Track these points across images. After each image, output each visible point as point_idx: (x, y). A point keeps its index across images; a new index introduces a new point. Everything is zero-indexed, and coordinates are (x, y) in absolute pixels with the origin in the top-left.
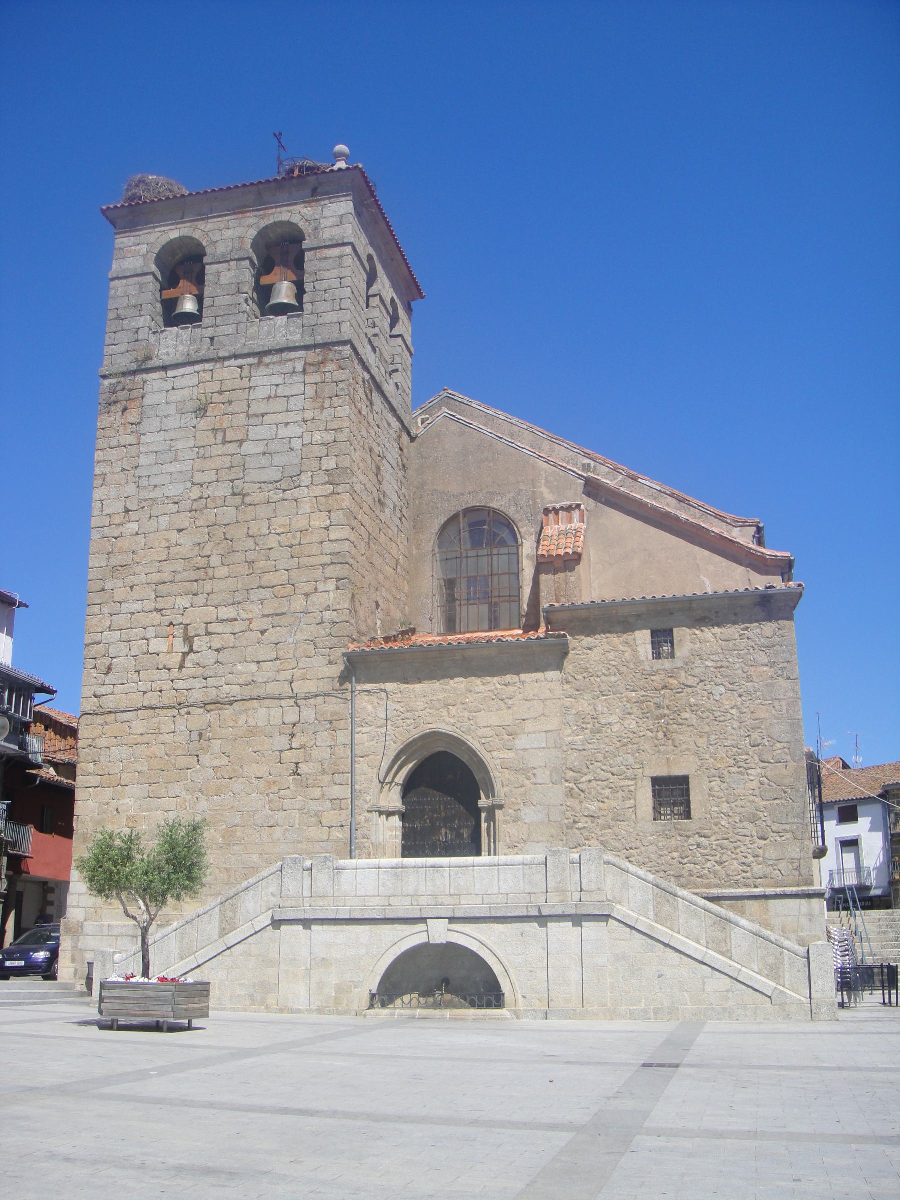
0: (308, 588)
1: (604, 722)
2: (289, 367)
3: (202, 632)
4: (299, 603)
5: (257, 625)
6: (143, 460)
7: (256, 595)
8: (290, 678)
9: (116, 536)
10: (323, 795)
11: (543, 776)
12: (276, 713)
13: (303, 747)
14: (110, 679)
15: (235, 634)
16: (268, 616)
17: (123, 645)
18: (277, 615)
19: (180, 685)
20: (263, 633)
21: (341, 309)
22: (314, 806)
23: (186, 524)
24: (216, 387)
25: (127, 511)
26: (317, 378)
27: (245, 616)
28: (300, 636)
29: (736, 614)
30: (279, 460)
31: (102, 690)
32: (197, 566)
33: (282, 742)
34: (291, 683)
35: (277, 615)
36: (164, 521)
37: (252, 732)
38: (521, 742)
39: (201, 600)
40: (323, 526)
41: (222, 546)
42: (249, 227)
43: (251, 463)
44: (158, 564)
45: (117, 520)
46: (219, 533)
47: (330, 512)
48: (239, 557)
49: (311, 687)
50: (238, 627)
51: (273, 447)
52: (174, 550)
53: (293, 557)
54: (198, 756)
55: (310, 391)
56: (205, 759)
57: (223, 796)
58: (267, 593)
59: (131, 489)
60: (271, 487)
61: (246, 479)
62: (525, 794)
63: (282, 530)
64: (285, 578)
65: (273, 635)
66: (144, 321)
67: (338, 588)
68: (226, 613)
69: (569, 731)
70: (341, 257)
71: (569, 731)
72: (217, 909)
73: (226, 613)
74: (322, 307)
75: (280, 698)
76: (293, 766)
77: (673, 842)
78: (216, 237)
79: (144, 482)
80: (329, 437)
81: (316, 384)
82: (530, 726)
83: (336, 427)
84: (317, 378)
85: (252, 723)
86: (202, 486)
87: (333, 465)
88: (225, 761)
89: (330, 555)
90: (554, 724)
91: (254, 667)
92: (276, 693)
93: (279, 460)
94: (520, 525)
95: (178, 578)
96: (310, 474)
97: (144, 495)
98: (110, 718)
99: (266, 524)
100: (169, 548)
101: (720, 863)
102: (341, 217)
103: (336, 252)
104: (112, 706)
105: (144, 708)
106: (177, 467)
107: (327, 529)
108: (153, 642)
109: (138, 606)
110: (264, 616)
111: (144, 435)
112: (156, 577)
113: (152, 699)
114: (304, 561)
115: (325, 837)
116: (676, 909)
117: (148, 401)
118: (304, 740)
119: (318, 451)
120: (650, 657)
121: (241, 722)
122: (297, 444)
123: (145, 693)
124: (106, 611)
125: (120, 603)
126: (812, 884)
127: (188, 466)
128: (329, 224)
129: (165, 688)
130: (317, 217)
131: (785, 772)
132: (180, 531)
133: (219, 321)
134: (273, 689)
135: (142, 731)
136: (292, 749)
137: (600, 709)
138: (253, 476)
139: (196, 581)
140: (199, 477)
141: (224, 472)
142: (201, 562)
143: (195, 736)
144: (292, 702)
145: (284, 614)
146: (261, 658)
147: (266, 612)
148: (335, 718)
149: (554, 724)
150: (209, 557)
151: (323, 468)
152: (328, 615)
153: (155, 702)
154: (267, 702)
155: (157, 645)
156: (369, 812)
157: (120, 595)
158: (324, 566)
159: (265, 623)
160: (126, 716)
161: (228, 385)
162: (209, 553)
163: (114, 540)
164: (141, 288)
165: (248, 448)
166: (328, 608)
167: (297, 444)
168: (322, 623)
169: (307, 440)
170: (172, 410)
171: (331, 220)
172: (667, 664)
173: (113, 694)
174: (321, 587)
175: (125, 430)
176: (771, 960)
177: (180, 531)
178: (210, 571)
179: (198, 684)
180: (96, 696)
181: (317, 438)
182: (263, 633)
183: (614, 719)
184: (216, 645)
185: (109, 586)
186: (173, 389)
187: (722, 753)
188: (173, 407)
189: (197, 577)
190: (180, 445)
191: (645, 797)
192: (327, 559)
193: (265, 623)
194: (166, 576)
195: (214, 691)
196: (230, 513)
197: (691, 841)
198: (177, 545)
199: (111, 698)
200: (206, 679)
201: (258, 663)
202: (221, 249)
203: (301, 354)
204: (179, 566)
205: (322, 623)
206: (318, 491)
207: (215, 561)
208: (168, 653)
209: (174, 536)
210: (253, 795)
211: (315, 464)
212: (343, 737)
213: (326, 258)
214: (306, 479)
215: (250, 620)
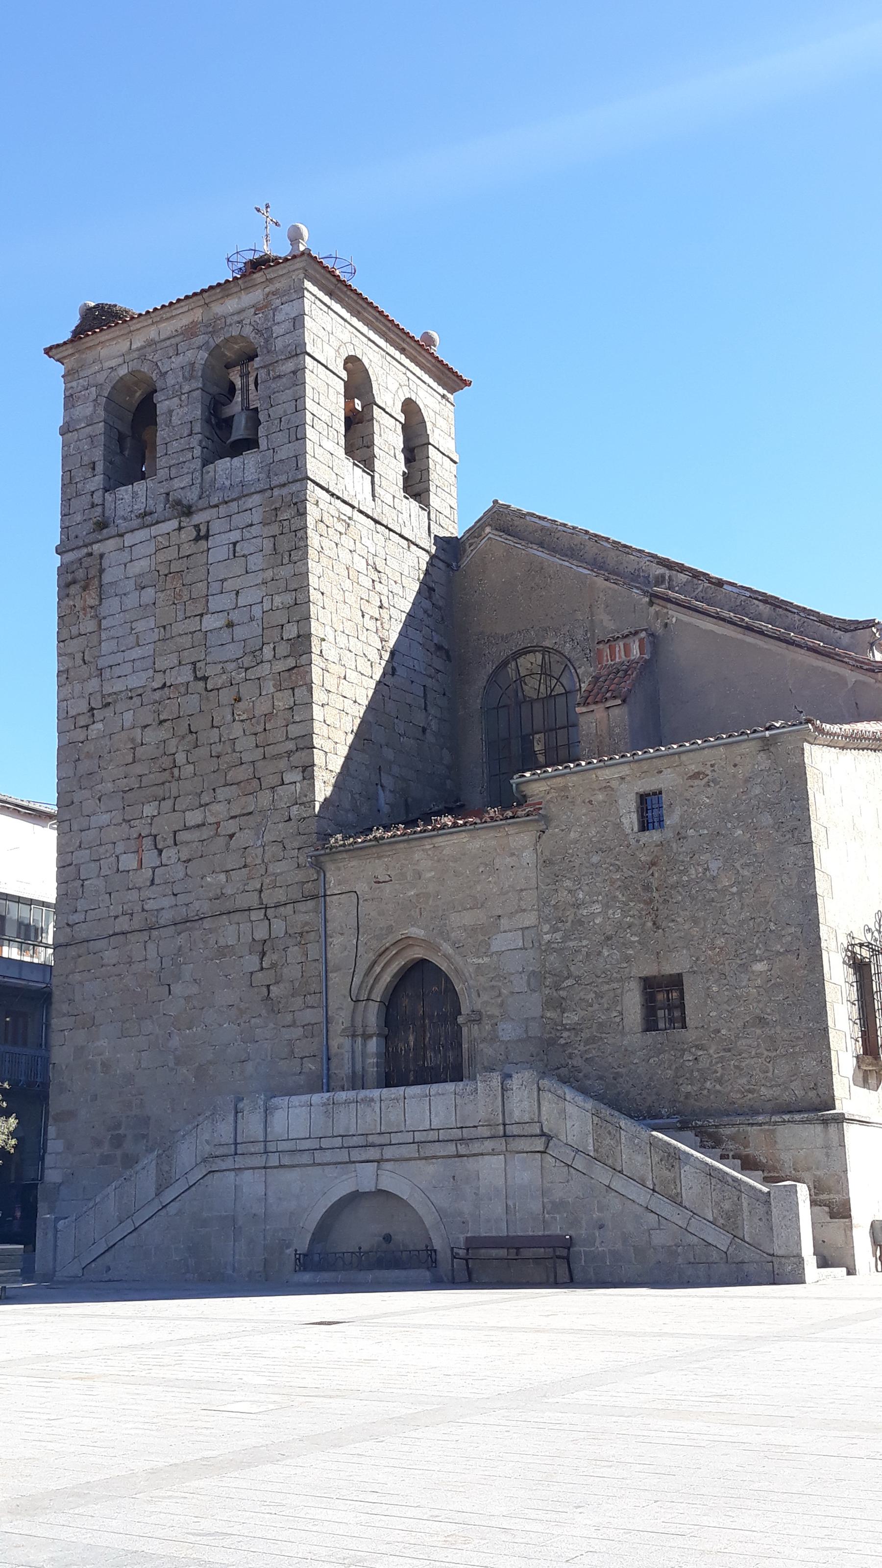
0: (274, 780)
2: (246, 518)
4: (265, 799)
6: (105, 647)
8: (259, 886)
9: (82, 740)
10: (294, 1021)
11: (520, 983)
13: (274, 966)
16: (232, 818)
17: (93, 865)
18: (244, 815)
20: (231, 836)
21: (297, 439)
22: (287, 1034)
24: (172, 553)
25: (92, 709)
26: (275, 529)
27: (211, 820)
28: (268, 837)
29: (735, 766)
31: (76, 918)
32: (163, 766)
33: (251, 962)
34: (261, 891)
35: (244, 815)
36: (128, 716)
37: (223, 951)
38: (499, 943)
39: (168, 804)
40: (287, 707)
41: (187, 740)
42: (200, 348)
43: (212, 639)
45: (82, 721)
48: (203, 751)
49: (280, 895)
50: (206, 833)
52: (140, 751)
53: (257, 746)
54: (169, 985)
55: (268, 545)
56: (177, 989)
57: (194, 1030)
59: (94, 683)
61: (208, 659)
63: (244, 717)
64: (251, 770)
66: (98, 481)
67: (304, 778)
68: (193, 818)
70: (294, 372)
72: (154, 1162)
73: (193, 818)
76: (265, 990)
79: (107, 674)
80: (288, 599)
82: (504, 922)
83: (296, 587)
84: (275, 529)
85: (222, 942)
86: (164, 672)
88: (195, 989)
91: (222, 877)
92: (245, 906)
93: (240, 632)
94: (577, 665)
96: (272, 645)
97: (107, 689)
98: (82, 949)
99: (228, 710)
100: (134, 749)
101: (719, 1081)
102: (294, 319)
103: (290, 366)
104: (84, 935)
106: (137, 653)
108: (123, 858)
109: (105, 818)
110: (232, 818)
111: (104, 618)
112: (123, 784)
113: (123, 924)
115: (298, 1069)
116: (619, 1142)
117: (107, 578)
118: (275, 957)
119: (280, 617)
120: (636, 829)
121: (212, 942)
122: (257, 611)
123: (116, 917)
126: (834, 1109)
127: (148, 650)
128: (282, 332)
131: (796, 963)
133: (174, 472)
134: (243, 901)
135: (114, 961)
136: (262, 969)
138: (216, 654)
141: (186, 653)
142: (166, 762)
143: (167, 962)
145: (250, 813)
146: (229, 867)
148: (307, 928)
149: (530, 919)
150: (174, 754)
152: (294, 810)
153: (126, 927)
154: (236, 917)
155: (129, 862)
157: (89, 805)
158: (289, 753)
159: (231, 826)
162: (174, 751)
163: (80, 744)
165: (210, 622)
167: (257, 611)
168: (290, 819)
169: (267, 606)
170: (130, 585)
172: (654, 836)
174: (288, 778)
175: (85, 614)
176: (727, 1206)
179: (167, 902)
182: (231, 836)
183: (597, 908)
184: (185, 855)
188: (132, 581)
189: (164, 779)
190: (140, 626)
192: (291, 746)
193: (231, 826)
194: (134, 783)
196: (191, 703)
198: (142, 744)
199: (84, 925)
200: (175, 895)
203: (257, 499)
205: (290, 819)
207: (181, 758)
210: (225, 1025)
212: (314, 951)
213: (279, 376)
214: (268, 652)
215: (218, 824)
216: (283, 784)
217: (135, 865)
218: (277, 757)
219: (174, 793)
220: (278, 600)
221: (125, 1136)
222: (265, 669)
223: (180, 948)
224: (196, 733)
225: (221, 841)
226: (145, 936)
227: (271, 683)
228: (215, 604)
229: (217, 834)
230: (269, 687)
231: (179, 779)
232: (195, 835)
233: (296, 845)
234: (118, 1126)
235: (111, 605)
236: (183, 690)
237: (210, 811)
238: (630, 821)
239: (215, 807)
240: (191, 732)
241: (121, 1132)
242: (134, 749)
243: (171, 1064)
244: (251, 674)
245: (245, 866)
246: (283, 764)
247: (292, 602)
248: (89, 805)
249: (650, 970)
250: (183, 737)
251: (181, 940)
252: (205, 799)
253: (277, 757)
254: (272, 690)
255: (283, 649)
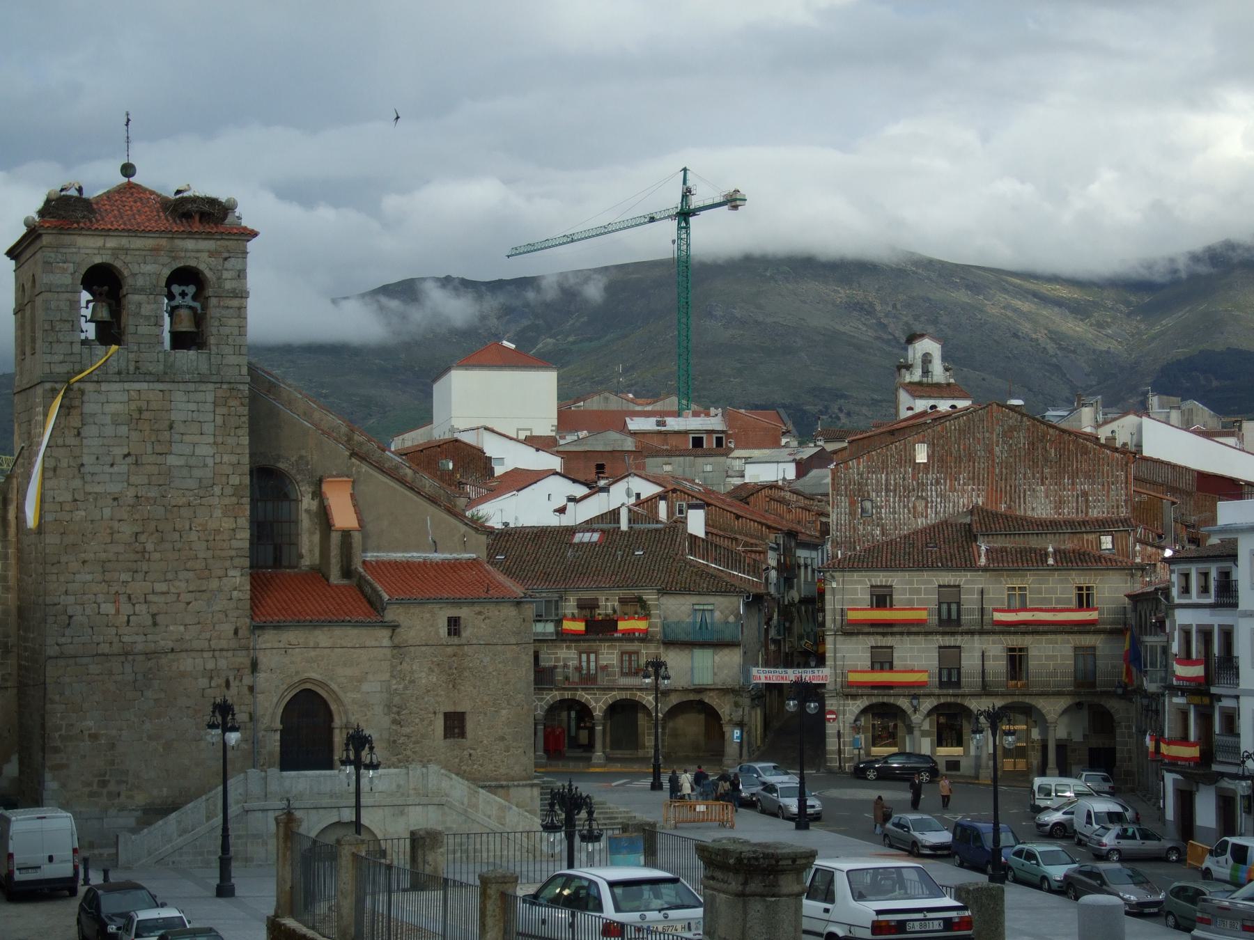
0: (220, 573)
1: (416, 676)
2: (200, 396)
3: (142, 600)
4: (214, 584)
5: (186, 597)
7: (182, 575)
12: (199, 661)
14: (67, 632)
15: (167, 603)
16: (189, 592)
17: (78, 607)
18: (199, 591)
19: (125, 639)
20: (188, 603)
23: (125, 517)
25: (75, 500)
28: (216, 608)
30: (197, 473)
31: (63, 640)
34: (210, 640)
35: (199, 591)
38: (366, 687)
39: (140, 576)
44: (103, 546)
46: (153, 525)
47: (235, 517)
51: (192, 461)
52: (116, 536)
55: (219, 420)
58: (191, 574)
60: (191, 493)
62: (367, 720)
64: (204, 564)
65: (195, 606)
67: (242, 575)
69: (394, 682)
70: (239, 308)
71: (394, 682)
74: (227, 350)
75: (202, 651)
77: (455, 752)
78: (135, 269)
81: (224, 415)
82: (370, 677)
85: (182, 668)
87: (237, 482)
88: (163, 695)
89: (236, 549)
90: (386, 676)
91: (182, 628)
95: (121, 558)
96: (221, 486)
105: (97, 655)
107: (234, 530)
108: (103, 606)
109: (89, 577)
110: (189, 592)
111: (86, 438)
112: (103, 556)
114: (218, 553)
122: (210, 461)
124: (62, 579)
125: (74, 574)
129: (114, 640)
130: (220, 268)
132: (120, 521)
134: (196, 644)
136: (210, 687)
137: (414, 668)
139: (136, 561)
140: (133, 479)
143: (140, 677)
144: (211, 654)
145: (204, 591)
147: (191, 589)
148: (242, 666)
151: (230, 483)
152: (235, 594)
154: (193, 654)
155: (108, 608)
156: (266, 731)
157: (74, 566)
158: (232, 558)
159: (189, 597)
160: (85, 660)
161: (154, 406)
164: (71, 305)
165: (172, 460)
166: (235, 589)
167: (210, 461)
169: (218, 460)
170: (108, 420)
171: (231, 272)
172: (455, 640)
173: (72, 643)
177: (120, 521)
178: (147, 556)
179: (140, 638)
180: (58, 644)
181: (226, 458)
182: (188, 603)
183: (423, 675)
185: (64, 559)
186: (107, 402)
187: (486, 698)
188: (109, 418)
191: (440, 724)
192: (233, 553)
193: (189, 597)
195: (153, 645)
197: (465, 752)
198: (119, 532)
199: (71, 646)
200: (145, 635)
201: (185, 625)
202: (140, 282)
203: (211, 386)
204: (121, 549)
205: (231, 599)
206: (227, 501)
207: (150, 547)
208: (115, 615)
209: (116, 525)
211: (224, 479)
213: (228, 307)
214: (217, 490)
216: (227, 576)
217: (113, 612)
218: (224, 558)
219: (145, 568)
220: (226, 458)
221: (109, 781)
222: (216, 501)
223: (150, 669)
224: (162, 532)
225: (182, 606)
226: (123, 658)
227: (220, 511)
228: (176, 448)
229: (178, 600)
230: (218, 513)
231: (149, 560)
232: (161, 599)
233: (235, 615)
234: (104, 775)
235: (90, 431)
236: (152, 502)
237: (173, 585)
238: (443, 631)
239: (177, 583)
240: (157, 531)
241: (107, 778)
242: (112, 534)
243: (145, 740)
244: (204, 501)
245: (199, 623)
246: (228, 563)
247: (236, 462)
248: (74, 566)
249: (450, 709)
250: (152, 534)
251: (150, 664)
252: (170, 576)
253: (224, 558)
254: (220, 515)
255: (228, 491)
